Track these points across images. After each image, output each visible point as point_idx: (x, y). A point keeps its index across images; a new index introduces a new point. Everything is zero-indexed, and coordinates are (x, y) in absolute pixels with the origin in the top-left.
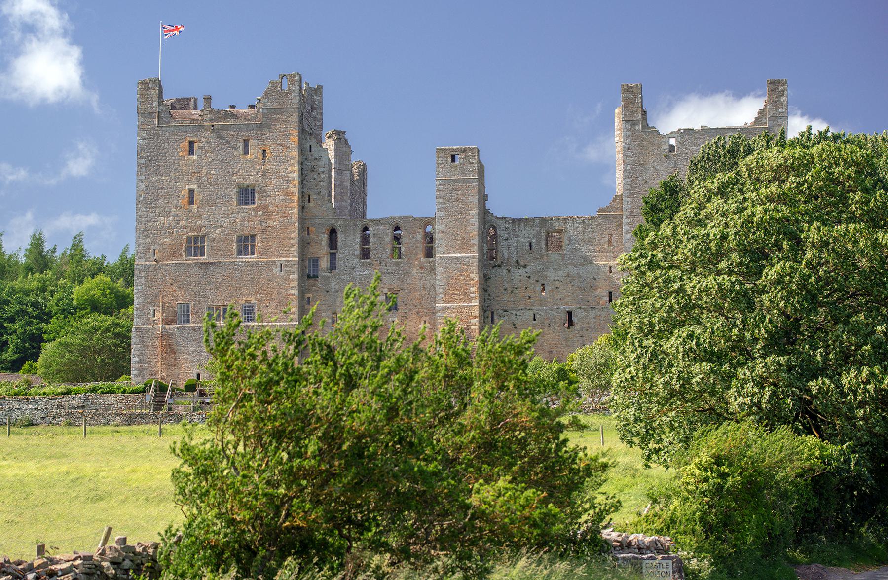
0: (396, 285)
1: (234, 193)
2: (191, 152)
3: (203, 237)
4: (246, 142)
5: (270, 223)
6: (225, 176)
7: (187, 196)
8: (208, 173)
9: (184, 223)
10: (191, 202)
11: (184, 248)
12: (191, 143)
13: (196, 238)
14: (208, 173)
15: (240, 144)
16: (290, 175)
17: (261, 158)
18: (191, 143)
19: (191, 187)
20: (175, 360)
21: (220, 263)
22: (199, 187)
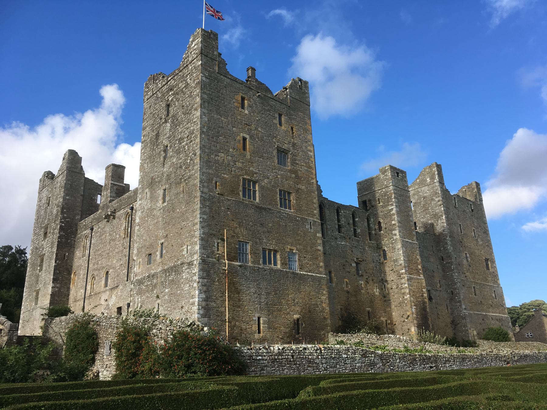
0: (359, 255)
1: (275, 152)
2: (243, 107)
3: (255, 183)
4: (280, 115)
5: (300, 186)
6: (268, 137)
7: (242, 142)
8: (256, 129)
9: (239, 165)
10: (244, 148)
11: (241, 188)
12: (243, 99)
13: (249, 181)
14: (256, 129)
15: (277, 115)
16: (309, 153)
17: (291, 132)
18: (243, 99)
19: (245, 135)
20: (239, 300)
21: (270, 209)
22: (251, 137)
